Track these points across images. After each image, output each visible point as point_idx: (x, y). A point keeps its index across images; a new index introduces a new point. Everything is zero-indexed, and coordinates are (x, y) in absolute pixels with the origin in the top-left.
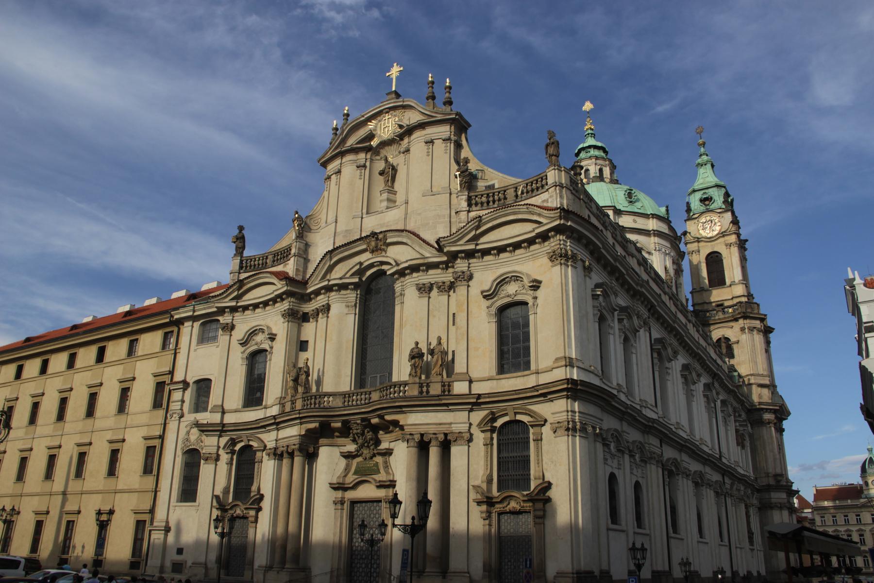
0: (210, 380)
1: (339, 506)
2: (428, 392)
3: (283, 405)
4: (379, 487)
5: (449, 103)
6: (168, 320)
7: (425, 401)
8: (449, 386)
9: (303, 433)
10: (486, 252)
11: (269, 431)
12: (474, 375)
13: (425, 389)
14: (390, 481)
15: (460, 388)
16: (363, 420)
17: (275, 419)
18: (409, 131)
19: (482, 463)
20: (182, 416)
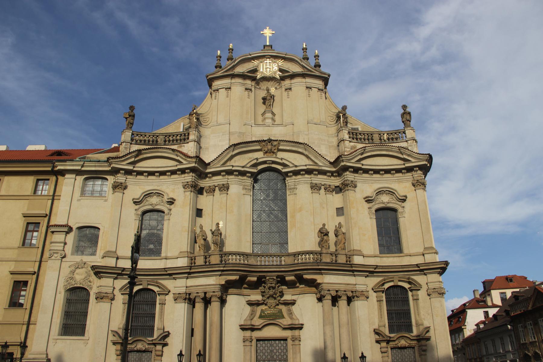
1: (248, 343)
3: (192, 259)
4: (285, 329)
5: (318, 66)
6: (50, 169)
7: (336, 268)
8: (349, 258)
9: (224, 283)
10: (366, 171)
11: (175, 279)
12: (365, 252)
16: (277, 277)
17: (190, 269)
18: (293, 76)
19: (377, 313)
20: (64, 257)
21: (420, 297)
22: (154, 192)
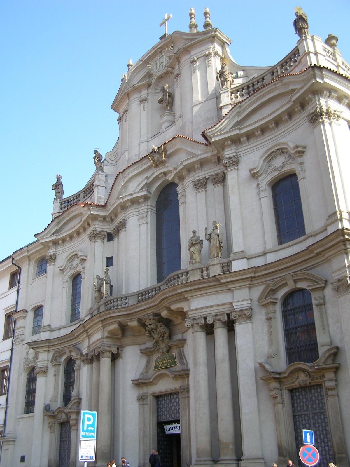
0: (43, 306)
2: (208, 275)
8: (228, 266)
9: (106, 334)
10: (249, 136)
13: (205, 273)
14: (183, 370)
15: (237, 266)
21: (327, 298)
22: (73, 254)
